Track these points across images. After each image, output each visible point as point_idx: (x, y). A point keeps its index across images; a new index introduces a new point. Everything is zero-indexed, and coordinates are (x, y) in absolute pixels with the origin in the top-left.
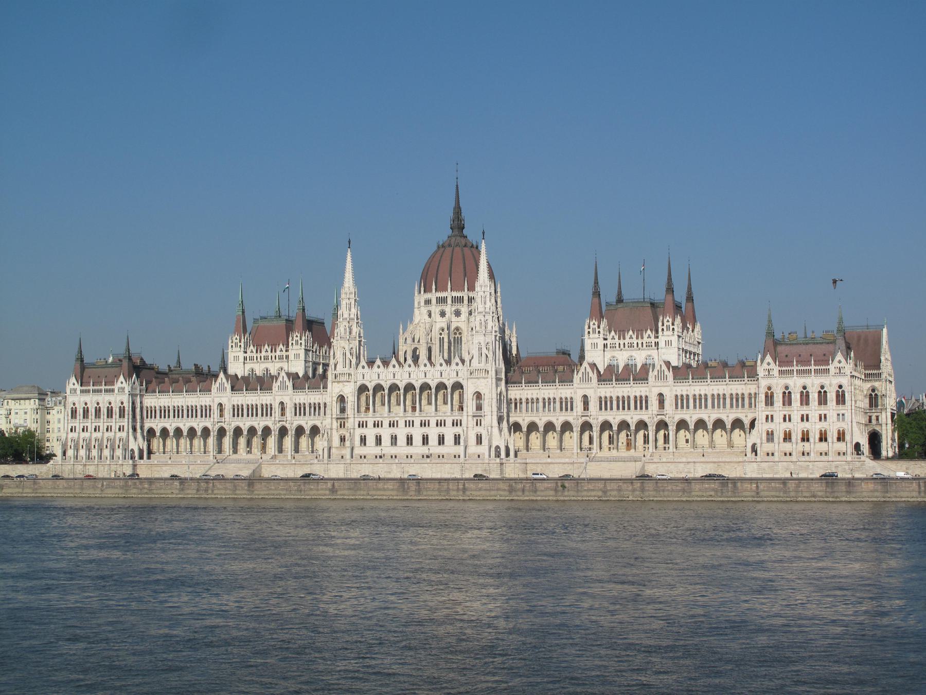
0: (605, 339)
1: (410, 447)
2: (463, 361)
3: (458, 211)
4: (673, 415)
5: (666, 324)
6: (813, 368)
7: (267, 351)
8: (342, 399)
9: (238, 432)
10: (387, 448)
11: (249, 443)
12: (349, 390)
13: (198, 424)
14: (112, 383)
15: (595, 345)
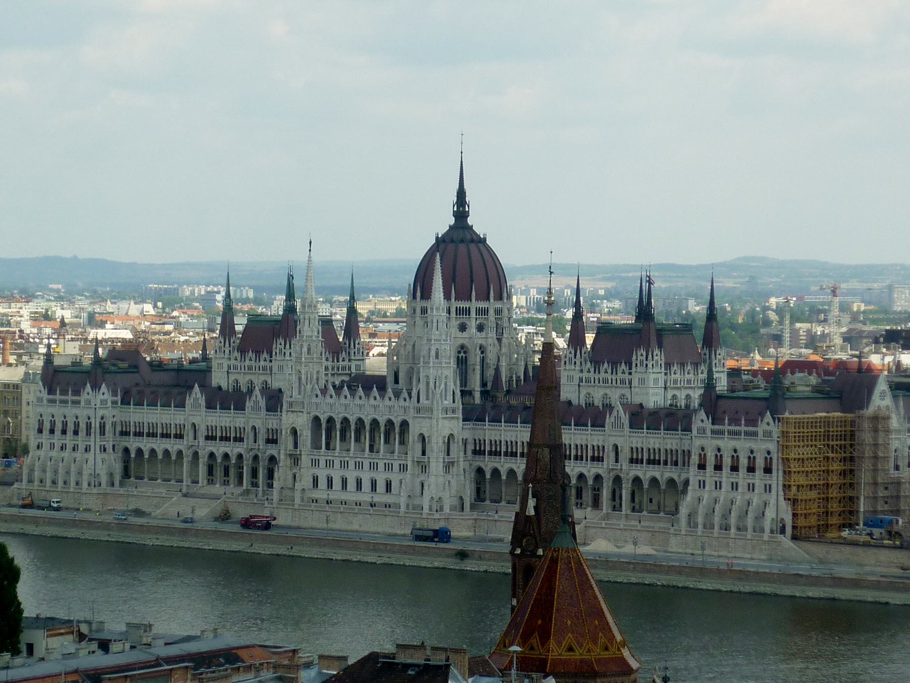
0: (582, 371)
1: (359, 493)
2: (410, 398)
3: (461, 194)
4: (629, 472)
5: (639, 358)
6: (743, 428)
7: (251, 360)
8: (294, 432)
9: (212, 455)
10: (337, 494)
11: (227, 473)
12: (302, 422)
13: (173, 446)
14: (77, 393)
15: (570, 378)
